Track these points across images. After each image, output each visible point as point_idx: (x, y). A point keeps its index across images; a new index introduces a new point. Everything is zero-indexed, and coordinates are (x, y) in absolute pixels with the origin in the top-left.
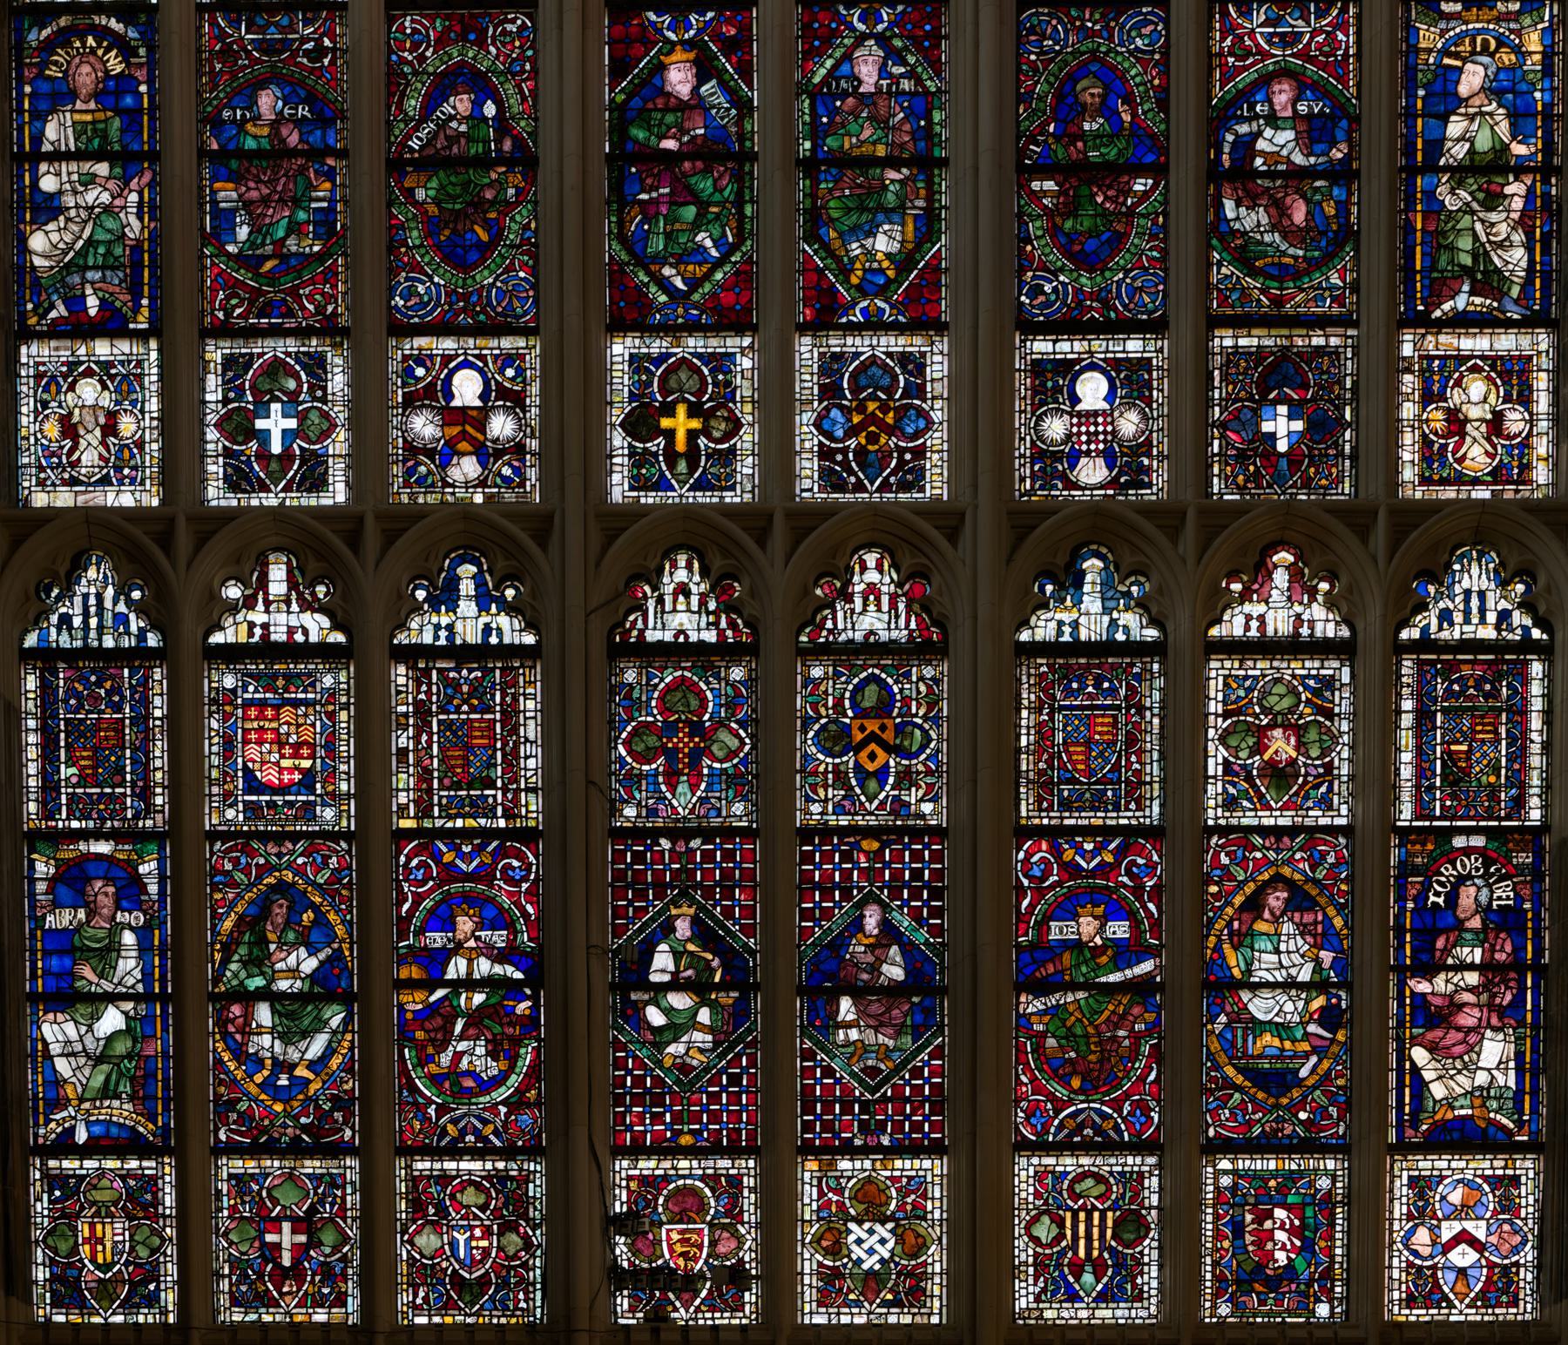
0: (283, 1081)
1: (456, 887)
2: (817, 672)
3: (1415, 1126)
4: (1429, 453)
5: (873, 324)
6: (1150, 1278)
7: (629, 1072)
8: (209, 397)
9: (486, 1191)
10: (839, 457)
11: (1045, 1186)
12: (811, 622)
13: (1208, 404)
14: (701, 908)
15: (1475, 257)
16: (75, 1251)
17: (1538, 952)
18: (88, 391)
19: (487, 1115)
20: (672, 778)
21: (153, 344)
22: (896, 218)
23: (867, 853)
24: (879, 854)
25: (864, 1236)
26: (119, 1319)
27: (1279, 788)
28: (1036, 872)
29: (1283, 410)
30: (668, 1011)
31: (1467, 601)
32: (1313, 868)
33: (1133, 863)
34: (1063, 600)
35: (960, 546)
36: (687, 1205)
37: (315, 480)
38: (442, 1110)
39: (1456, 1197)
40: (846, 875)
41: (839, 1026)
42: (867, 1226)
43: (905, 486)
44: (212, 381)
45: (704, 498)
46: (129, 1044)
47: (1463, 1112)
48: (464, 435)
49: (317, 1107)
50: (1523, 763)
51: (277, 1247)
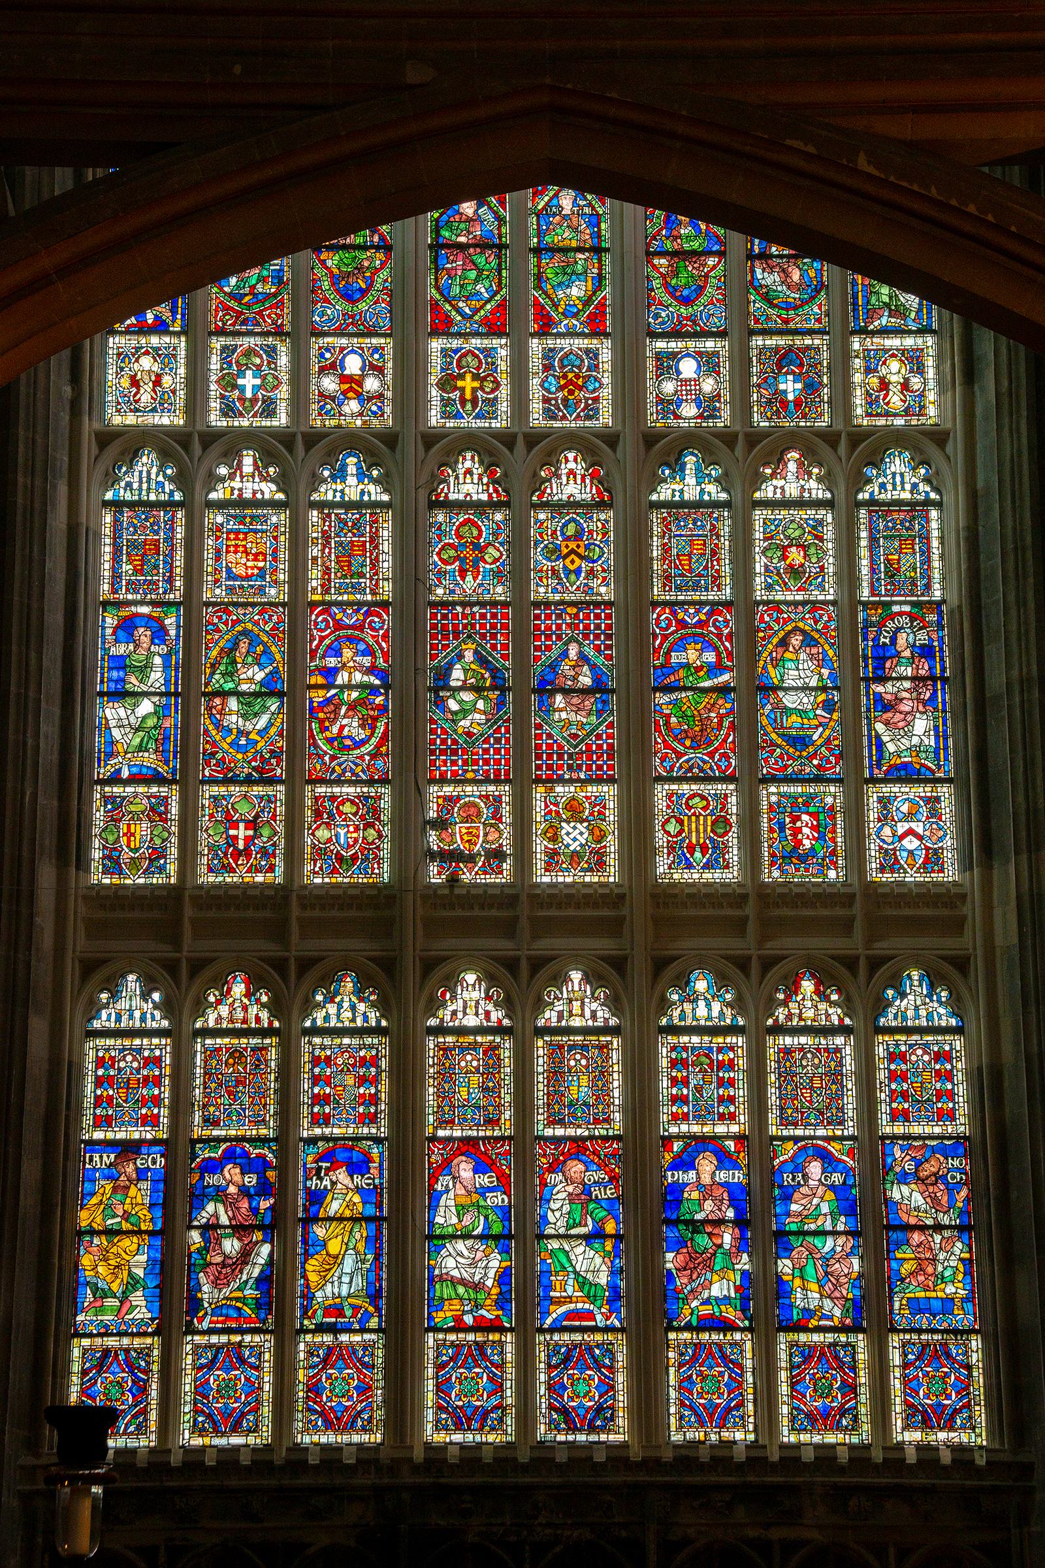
0: (243, 742)
1: (342, 633)
2: (542, 516)
3: (879, 768)
4: (871, 401)
5: (571, 334)
6: (734, 855)
7: (438, 736)
8: (212, 367)
9: (357, 805)
10: (553, 402)
11: (672, 802)
12: (539, 489)
13: (750, 375)
14: (479, 645)
15: (891, 298)
16: (117, 840)
17: (943, 669)
18: (146, 362)
19: (358, 761)
20: (463, 573)
21: (183, 339)
22: (582, 278)
23: (570, 615)
24: (576, 616)
25: (571, 830)
26: (141, 881)
27: (795, 579)
28: (663, 625)
29: (790, 377)
30: (461, 702)
31: (894, 478)
32: (816, 622)
33: (716, 620)
34: (674, 478)
35: (620, 448)
36: (471, 813)
37: (269, 410)
38: (333, 758)
39: (905, 808)
40: (559, 627)
41: (555, 711)
42: (572, 824)
43: (588, 418)
44: (214, 359)
45: (480, 423)
46: (155, 720)
47: (906, 760)
48: (351, 389)
49: (262, 756)
50: (929, 566)
51: (236, 838)
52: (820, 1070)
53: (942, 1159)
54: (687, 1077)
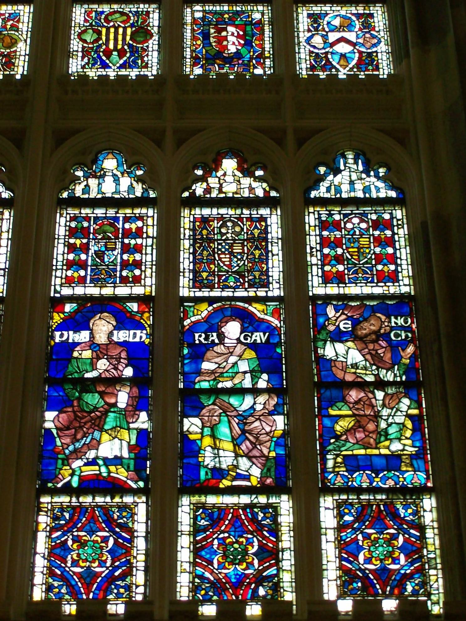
52: (241, 237)
53: (383, 318)
54: (88, 244)
